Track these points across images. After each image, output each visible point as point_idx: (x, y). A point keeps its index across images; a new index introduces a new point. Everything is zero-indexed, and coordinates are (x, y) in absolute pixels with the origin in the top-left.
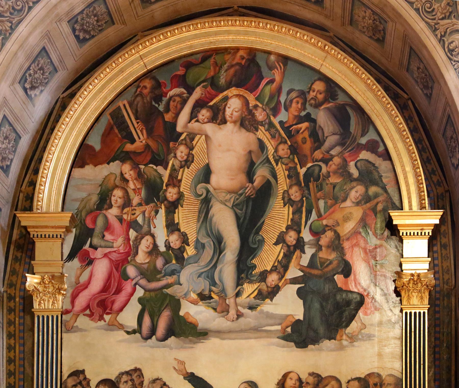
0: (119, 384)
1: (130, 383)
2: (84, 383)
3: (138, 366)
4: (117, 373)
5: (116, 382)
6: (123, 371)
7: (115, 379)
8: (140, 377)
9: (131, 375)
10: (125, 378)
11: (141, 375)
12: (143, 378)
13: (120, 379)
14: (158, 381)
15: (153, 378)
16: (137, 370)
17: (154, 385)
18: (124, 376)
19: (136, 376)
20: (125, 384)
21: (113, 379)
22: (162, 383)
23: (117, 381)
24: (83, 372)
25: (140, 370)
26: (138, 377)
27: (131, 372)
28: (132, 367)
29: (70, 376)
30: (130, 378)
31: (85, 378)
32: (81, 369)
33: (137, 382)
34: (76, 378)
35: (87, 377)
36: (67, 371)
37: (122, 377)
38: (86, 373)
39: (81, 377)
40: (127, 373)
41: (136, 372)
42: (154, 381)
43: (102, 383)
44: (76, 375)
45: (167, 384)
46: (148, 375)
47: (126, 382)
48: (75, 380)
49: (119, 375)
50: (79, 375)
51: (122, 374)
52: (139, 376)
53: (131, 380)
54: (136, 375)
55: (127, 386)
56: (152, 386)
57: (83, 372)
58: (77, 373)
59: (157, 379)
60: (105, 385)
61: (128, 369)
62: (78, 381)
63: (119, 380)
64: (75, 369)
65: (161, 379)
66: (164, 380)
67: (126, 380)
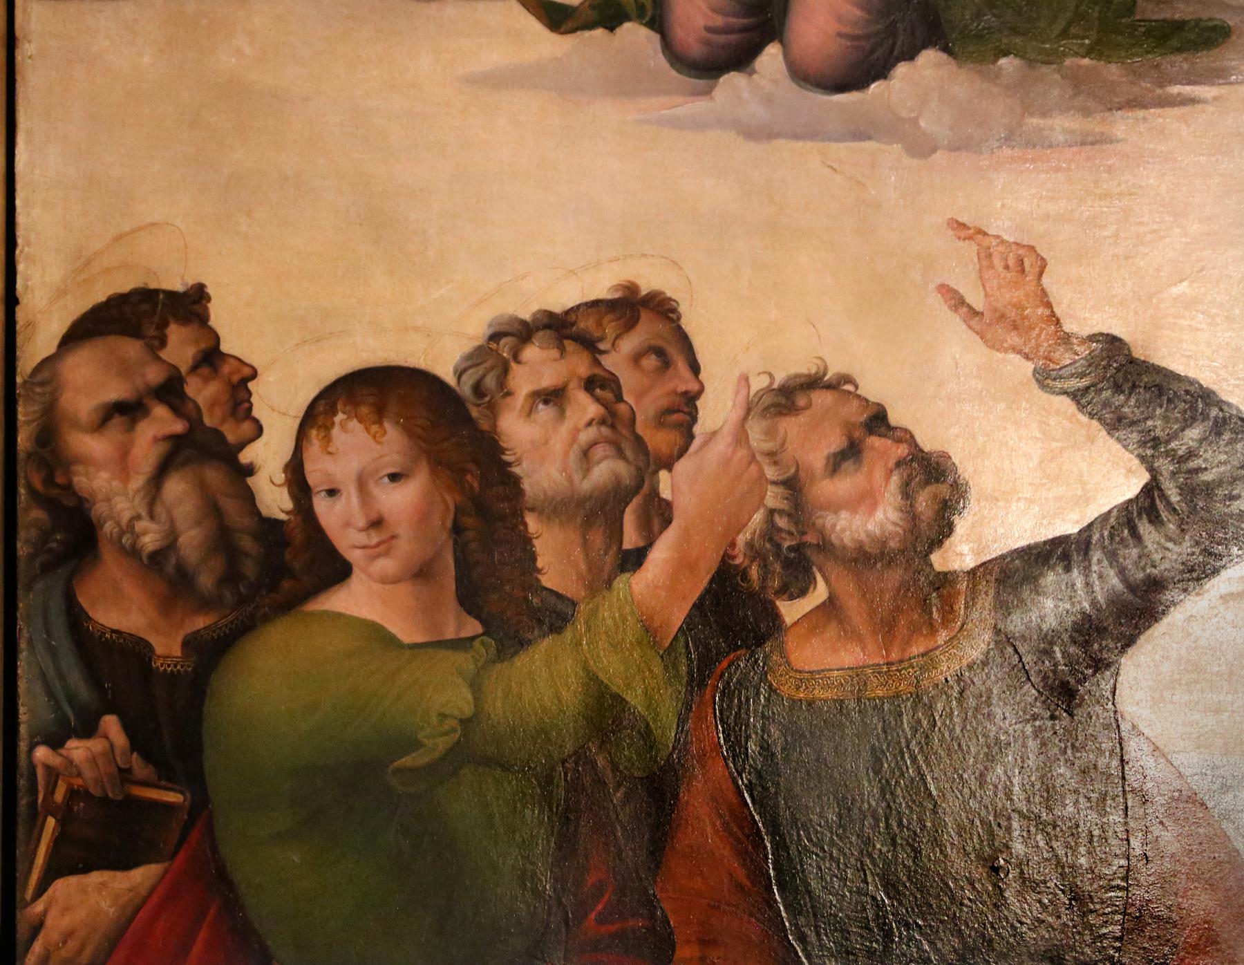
0: (493, 410)
1: (585, 407)
2: (202, 392)
3: (651, 278)
4: (476, 329)
5: (466, 390)
6: (526, 314)
7: (460, 374)
8: (666, 363)
9: (589, 344)
10: (539, 366)
11: (674, 347)
12: (695, 368)
13: (505, 370)
14: (821, 399)
15: (780, 378)
16: (631, 306)
17: (790, 426)
18: (531, 353)
19: (636, 358)
20: (544, 412)
21: (445, 371)
22: (854, 413)
23: (478, 389)
24: (191, 305)
25: (662, 308)
26: (651, 362)
27: (586, 324)
28: (601, 287)
29: (83, 331)
30: (580, 365)
31: (211, 357)
32: (179, 287)
33: (643, 398)
34: (132, 348)
35: (225, 347)
36: (61, 293)
37: (516, 357)
38: (219, 316)
39: (180, 347)
40: (559, 327)
41: (630, 324)
42: (787, 398)
43: (353, 402)
44: (133, 331)
45: (894, 418)
46: (735, 353)
47: (554, 397)
48: (125, 370)
49: (495, 337)
50: (163, 325)
51: (521, 332)
52: (660, 352)
53: (590, 385)
54: (630, 343)
55: (564, 430)
56: (770, 433)
57: (191, 305)
58: (144, 315)
59: (813, 383)
60: (380, 413)
61: (564, 297)
62: (154, 375)
63: (490, 382)
64: (124, 284)
65: (848, 379)
66: (872, 389)
67: (548, 380)
